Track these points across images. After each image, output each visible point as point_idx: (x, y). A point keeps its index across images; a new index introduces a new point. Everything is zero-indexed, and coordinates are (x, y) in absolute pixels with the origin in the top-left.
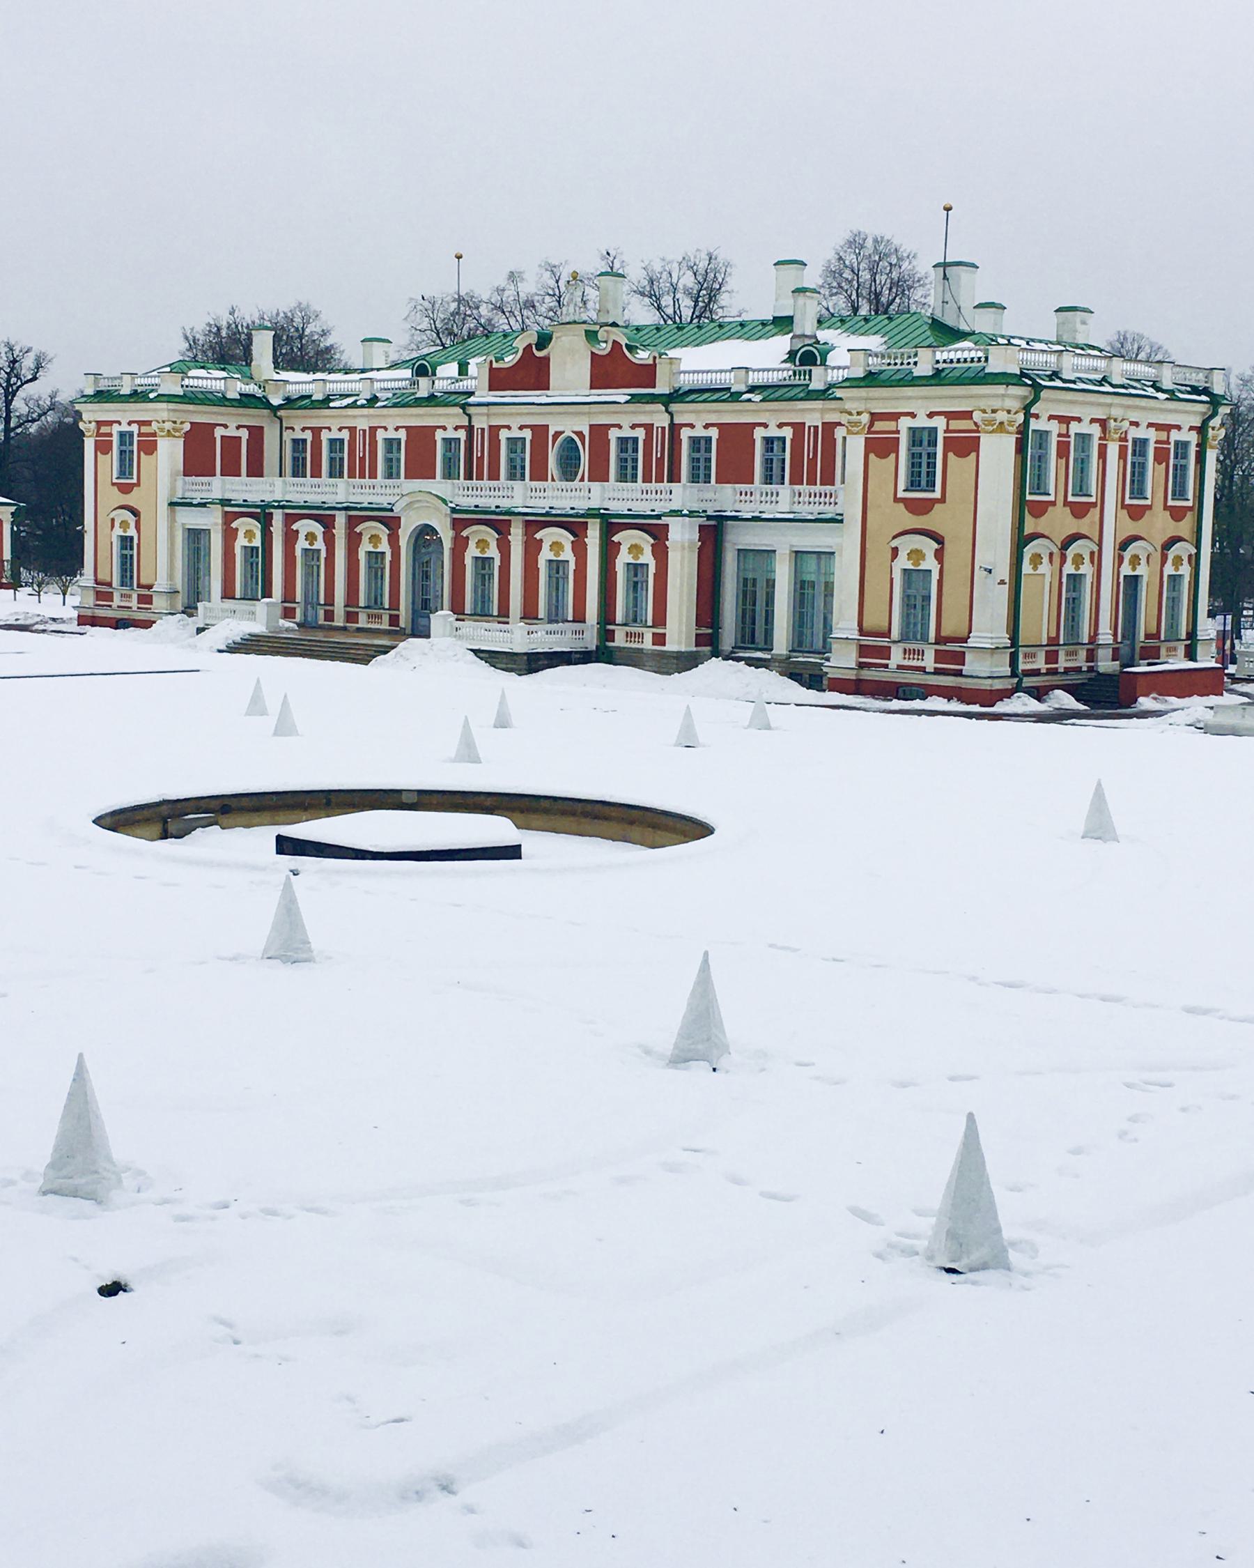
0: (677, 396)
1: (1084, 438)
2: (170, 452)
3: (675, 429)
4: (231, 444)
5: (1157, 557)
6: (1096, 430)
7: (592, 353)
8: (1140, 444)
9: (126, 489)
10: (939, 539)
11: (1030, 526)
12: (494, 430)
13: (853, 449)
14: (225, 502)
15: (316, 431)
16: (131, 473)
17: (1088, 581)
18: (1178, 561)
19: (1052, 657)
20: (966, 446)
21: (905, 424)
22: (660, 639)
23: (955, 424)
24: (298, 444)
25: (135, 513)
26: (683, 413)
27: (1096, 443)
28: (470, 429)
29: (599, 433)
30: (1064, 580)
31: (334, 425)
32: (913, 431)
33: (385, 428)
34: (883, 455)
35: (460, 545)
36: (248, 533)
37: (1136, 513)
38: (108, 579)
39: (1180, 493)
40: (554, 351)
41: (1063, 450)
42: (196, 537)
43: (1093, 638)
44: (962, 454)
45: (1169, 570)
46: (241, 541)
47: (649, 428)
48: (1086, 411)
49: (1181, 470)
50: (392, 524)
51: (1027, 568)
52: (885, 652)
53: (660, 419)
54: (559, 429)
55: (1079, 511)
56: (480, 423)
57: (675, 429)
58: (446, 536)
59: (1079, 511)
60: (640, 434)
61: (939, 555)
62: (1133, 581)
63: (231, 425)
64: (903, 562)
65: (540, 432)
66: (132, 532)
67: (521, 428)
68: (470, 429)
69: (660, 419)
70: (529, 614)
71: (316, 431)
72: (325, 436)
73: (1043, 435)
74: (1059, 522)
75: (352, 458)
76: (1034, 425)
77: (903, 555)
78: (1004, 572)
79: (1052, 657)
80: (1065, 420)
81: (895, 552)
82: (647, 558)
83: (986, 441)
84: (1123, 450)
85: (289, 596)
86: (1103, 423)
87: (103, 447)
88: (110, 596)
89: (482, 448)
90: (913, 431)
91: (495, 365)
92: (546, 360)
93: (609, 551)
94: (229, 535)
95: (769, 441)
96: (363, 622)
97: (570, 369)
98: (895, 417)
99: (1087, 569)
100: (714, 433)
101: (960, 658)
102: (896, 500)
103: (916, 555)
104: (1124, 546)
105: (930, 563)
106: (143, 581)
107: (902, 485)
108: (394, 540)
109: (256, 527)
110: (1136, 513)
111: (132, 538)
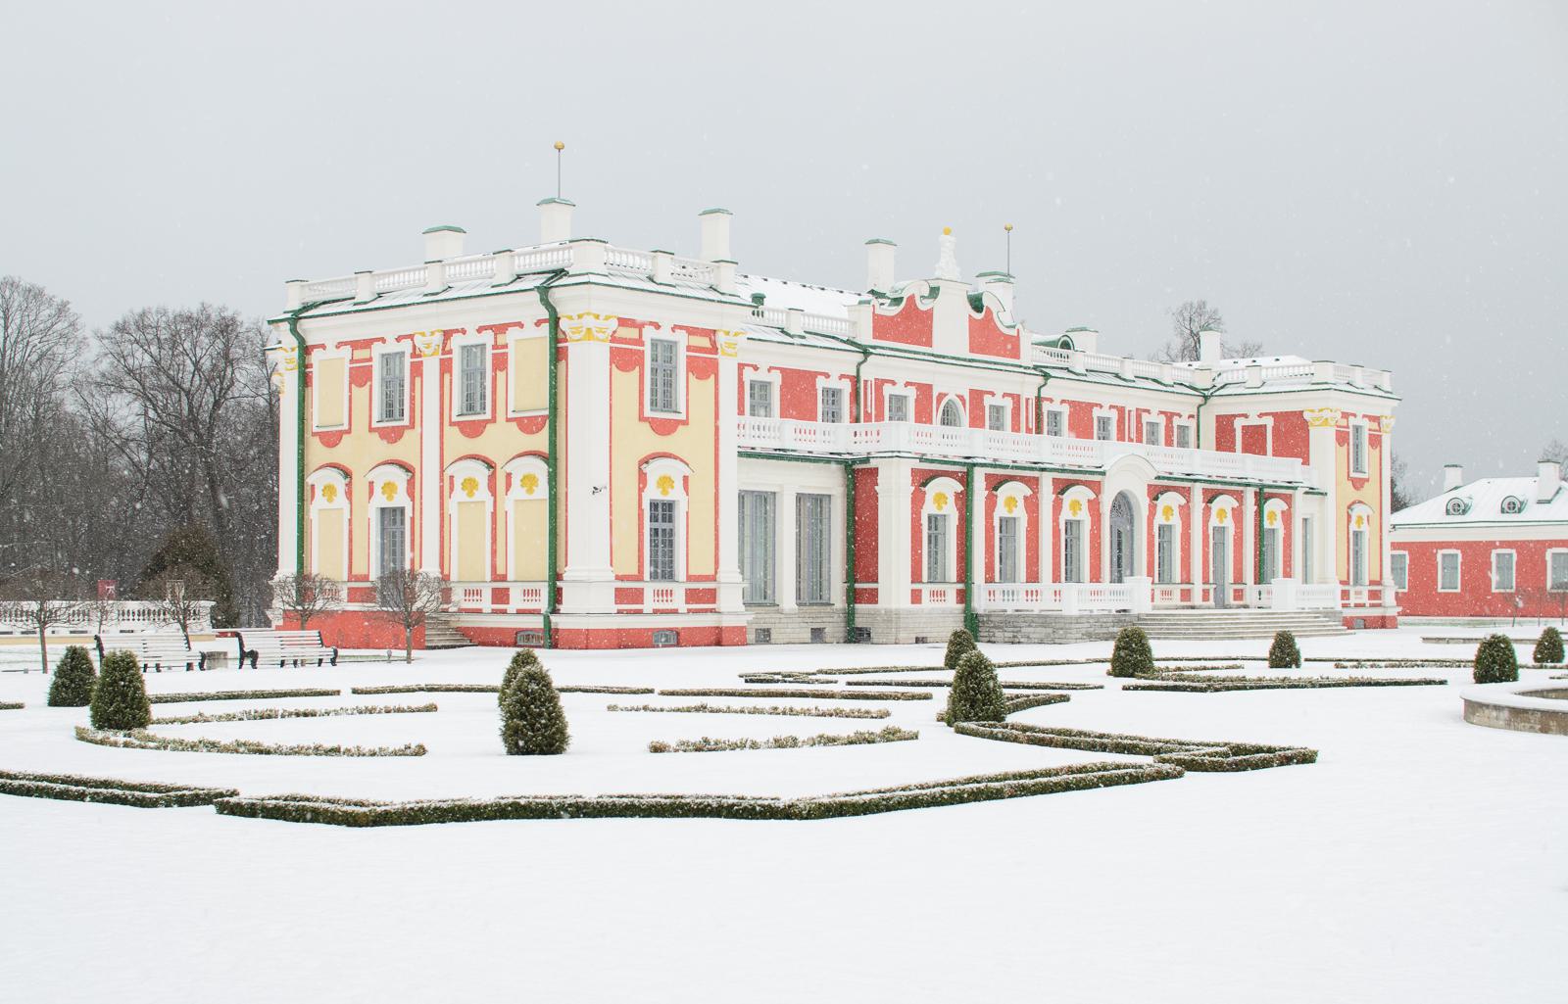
3: (1039, 400)
12: (880, 383)
16: (668, 405)
21: (1352, 421)
28: (855, 380)
29: (977, 396)
33: (756, 368)
38: (634, 571)
47: (1016, 398)
50: (1096, 487)
54: (944, 391)
58: (1142, 502)
60: (1008, 403)
65: (924, 390)
66: (676, 494)
68: (855, 380)
88: (637, 596)
92: (929, 314)
97: (951, 328)
100: (1065, 410)
106: (690, 573)
108: (1094, 507)
111: (669, 506)
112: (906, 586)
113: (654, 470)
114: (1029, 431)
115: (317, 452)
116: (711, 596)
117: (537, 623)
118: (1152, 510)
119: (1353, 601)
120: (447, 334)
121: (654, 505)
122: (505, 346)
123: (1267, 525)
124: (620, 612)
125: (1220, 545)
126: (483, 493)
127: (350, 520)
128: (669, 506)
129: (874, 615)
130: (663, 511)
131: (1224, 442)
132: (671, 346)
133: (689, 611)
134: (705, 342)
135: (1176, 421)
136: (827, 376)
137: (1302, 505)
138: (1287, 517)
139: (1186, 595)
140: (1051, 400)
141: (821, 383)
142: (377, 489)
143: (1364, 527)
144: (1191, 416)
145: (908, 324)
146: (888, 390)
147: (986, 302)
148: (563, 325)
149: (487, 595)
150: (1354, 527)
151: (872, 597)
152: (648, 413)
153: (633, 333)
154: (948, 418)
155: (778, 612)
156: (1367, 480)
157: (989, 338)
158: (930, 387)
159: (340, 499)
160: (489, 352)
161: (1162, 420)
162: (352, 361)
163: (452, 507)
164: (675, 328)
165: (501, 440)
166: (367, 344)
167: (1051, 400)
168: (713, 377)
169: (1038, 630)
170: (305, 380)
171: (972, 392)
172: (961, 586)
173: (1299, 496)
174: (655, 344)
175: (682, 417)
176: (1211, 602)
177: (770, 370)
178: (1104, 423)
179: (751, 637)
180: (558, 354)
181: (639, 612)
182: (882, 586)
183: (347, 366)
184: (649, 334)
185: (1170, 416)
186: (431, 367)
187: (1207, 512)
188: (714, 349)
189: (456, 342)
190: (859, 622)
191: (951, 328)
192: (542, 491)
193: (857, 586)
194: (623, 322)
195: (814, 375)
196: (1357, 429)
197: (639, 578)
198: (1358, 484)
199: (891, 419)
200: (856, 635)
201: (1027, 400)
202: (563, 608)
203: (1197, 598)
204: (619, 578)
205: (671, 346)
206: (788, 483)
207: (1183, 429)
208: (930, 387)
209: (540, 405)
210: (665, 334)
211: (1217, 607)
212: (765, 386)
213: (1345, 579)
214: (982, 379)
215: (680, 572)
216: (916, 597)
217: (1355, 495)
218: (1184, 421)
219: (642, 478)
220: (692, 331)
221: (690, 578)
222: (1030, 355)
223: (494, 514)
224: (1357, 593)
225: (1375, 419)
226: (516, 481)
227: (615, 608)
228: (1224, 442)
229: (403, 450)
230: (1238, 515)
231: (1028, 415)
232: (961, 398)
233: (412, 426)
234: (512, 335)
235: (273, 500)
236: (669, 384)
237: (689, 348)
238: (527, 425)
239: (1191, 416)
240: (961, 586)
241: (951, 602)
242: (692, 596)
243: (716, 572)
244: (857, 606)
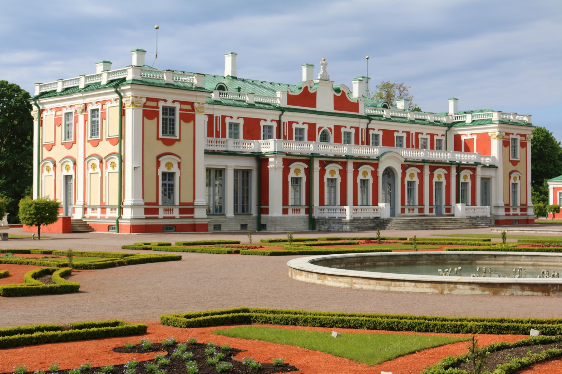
3: (368, 129)
7: (334, 95)
12: (291, 123)
16: (173, 132)
21: (511, 136)
25: (179, 157)
28: (279, 122)
29: (338, 129)
30: (511, 185)
36: (298, 170)
38: (154, 201)
44: (523, 147)
47: (357, 129)
50: (376, 166)
53: (362, 124)
54: (321, 126)
57: (368, 129)
60: (353, 131)
65: (312, 126)
66: (175, 169)
67: (304, 123)
68: (279, 122)
69: (362, 124)
81: (510, 178)
88: (156, 211)
91: (290, 93)
100: (381, 133)
102: (510, 161)
106: (182, 201)
108: (375, 174)
111: (172, 175)
112: (280, 207)
113: (164, 161)
114: (363, 143)
115: (46, 154)
116: (192, 211)
117: (113, 222)
119: (512, 212)
120: (86, 105)
121: (164, 174)
122: (105, 110)
123: (462, 180)
124: (147, 218)
125: (438, 190)
126: (98, 170)
127: (55, 180)
128: (172, 175)
129: (267, 219)
130: (169, 176)
131: (457, 148)
132: (173, 110)
133: (181, 218)
134: (189, 107)
135: (436, 138)
136: (265, 120)
137: (480, 172)
138: (473, 178)
139: (421, 210)
140: (374, 129)
141: (262, 123)
142: (64, 168)
143: (518, 181)
144: (442, 135)
146: (294, 126)
147: (341, 89)
148: (124, 100)
149: (99, 210)
150: (512, 181)
151: (266, 211)
152: (161, 136)
153: (154, 104)
154: (324, 138)
155: (225, 218)
156: (519, 161)
157: (343, 103)
158: (315, 125)
159: (52, 173)
160: (100, 111)
161: (429, 137)
162: (56, 115)
163: (88, 176)
164: (174, 102)
165: (105, 148)
166: (59, 109)
167: (374, 129)
168: (192, 122)
169: (337, 225)
170: (40, 124)
171: (335, 126)
172: (307, 207)
173: (479, 169)
174: (165, 109)
175: (178, 138)
176: (434, 213)
177: (238, 118)
178: (400, 138)
179: (211, 228)
180: (122, 113)
181: (157, 218)
182: (270, 207)
183: (53, 117)
184: (161, 104)
185: (432, 136)
186: (81, 118)
187: (431, 176)
188: (193, 110)
189: (90, 108)
190: (263, 222)
192: (117, 169)
193: (262, 207)
194: (148, 99)
195: (259, 120)
196: (515, 140)
197: (157, 203)
198: (514, 163)
199: (296, 138)
200: (261, 228)
201: (362, 129)
202: (124, 216)
203: (427, 212)
204: (146, 204)
205: (173, 110)
206: (231, 165)
207: (439, 141)
208: (315, 125)
209: (115, 133)
210: (169, 104)
211: (437, 215)
212: (237, 125)
213: (508, 203)
214: (340, 121)
215: (177, 203)
216: (285, 211)
217: (513, 168)
218: (439, 137)
219: (158, 164)
220: (182, 103)
221: (181, 204)
222: (362, 111)
223: (102, 177)
224: (513, 209)
225: (524, 136)
226: (109, 165)
227: (144, 216)
228: (457, 148)
229: (71, 152)
230: (448, 177)
231: (362, 136)
232: (330, 129)
233: (75, 142)
234: (108, 104)
235: (32, 173)
236: (173, 124)
237: (181, 110)
238: (112, 141)
239: (442, 135)
240: (307, 207)
241: (303, 213)
242: (181, 211)
243: (194, 201)
244: (262, 215)
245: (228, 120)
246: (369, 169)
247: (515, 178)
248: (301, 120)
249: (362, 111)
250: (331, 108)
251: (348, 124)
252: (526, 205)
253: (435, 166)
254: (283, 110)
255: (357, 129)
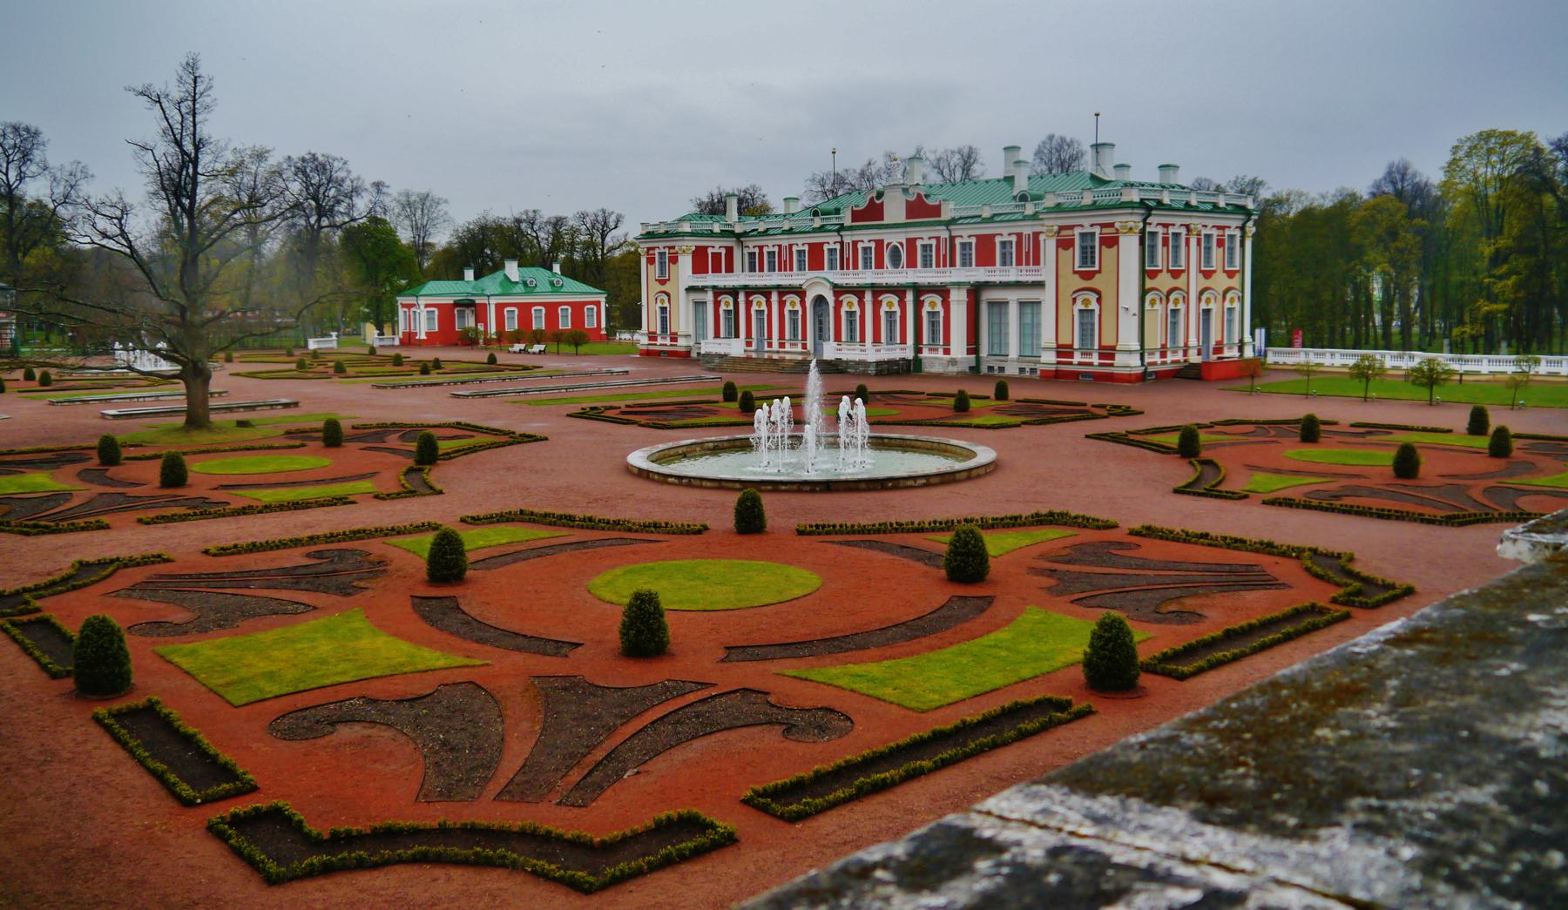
0: (953, 221)
1: (1176, 235)
2: (686, 262)
3: (952, 239)
4: (716, 256)
5: (1220, 298)
6: (1183, 231)
8: (1208, 237)
9: (663, 282)
10: (1098, 292)
11: (1149, 283)
12: (855, 243)
13: (1049, 247)
14: (714, 287)
15: (761, 248)
17: (1182, 312)
18: (1232, 301)
19: (1163, 355)
20: (1111, 242)
22: (947, 352)
23: (1105, 230)
24: (752, 255)
26: (956, 230)
27: (1183, 238)
28: (842, 243)
29: (911, 243)
31: (770, 245)
32: (1082, 235)
34: (1066, 248)
35: (838, 305)
36: (727, 302)
37: (1207, 275)
39: (1231, 262)
40: (885, 199)
41: (1165, 242)
42: (700, 305)
43: (1186, 345)
45: (1227, 305)
46: (723, 307)
47: (938, 238)
48: (1178, 222)
49: (1231, 249)
51: (1147, 306)
52: (1071, 355)
53: (944, 235)
55: (1175, 274)
56: (847, 240)
57: (952, 239)
58: (831, 299)
59: (1175, 274)
60: (934, 242)
61: (1099, 301)
62: (1207, 312)
63: (716, 246)
64: (1079, 306)
65: (879, 243)
66: (666, 304)
68: (842, 243)
70: (876, 340)
71: (761, 248)
72: (765, 250)
73: (1153, 234)
74: (1164, 282)
75: (781, 261)
76: (1149, 229)
77: (1079, 302)
78: (1135, 308)
79: (1163, 355)
80: (1166, 226)
81: (1074, 300)
82: (939, 308)
83: (1122, 240)
84: (1199, 241)
85: (749, 334)
86: (1187, 227)
87: (651, 261)
89: (848, 253)
90: (1082, 235)
93: (918, 305)
94: (717, 304)
95: (1003, 244)
96: (788, 348)
98: (1071, 227)
99: (1181, 306)
100: (973, 240)
101: (1112, 357)
103: (1086, 302)
104: (1201, 293)
105: (1094, 306)
107: (1077, 263)
108: (803, 303)
109: (730, 300)
110: (1207, 275)
118: (838, 305)
119: (1077, 358)
145: (872, 213)
146: (860, 246)
157: (920, 209)
171: (908, 240)
191: (894, 210)
195: (822, 244)
245: (795, 249)
246: (792, 299)
247: (1086, 302)
248: (866, 238)
249: (945, 216)
250: (902, 219)
251: (925, 236)
252: (1113, 348)
253: (878, 290)
254: (842, 228)
255: (938, 238)
